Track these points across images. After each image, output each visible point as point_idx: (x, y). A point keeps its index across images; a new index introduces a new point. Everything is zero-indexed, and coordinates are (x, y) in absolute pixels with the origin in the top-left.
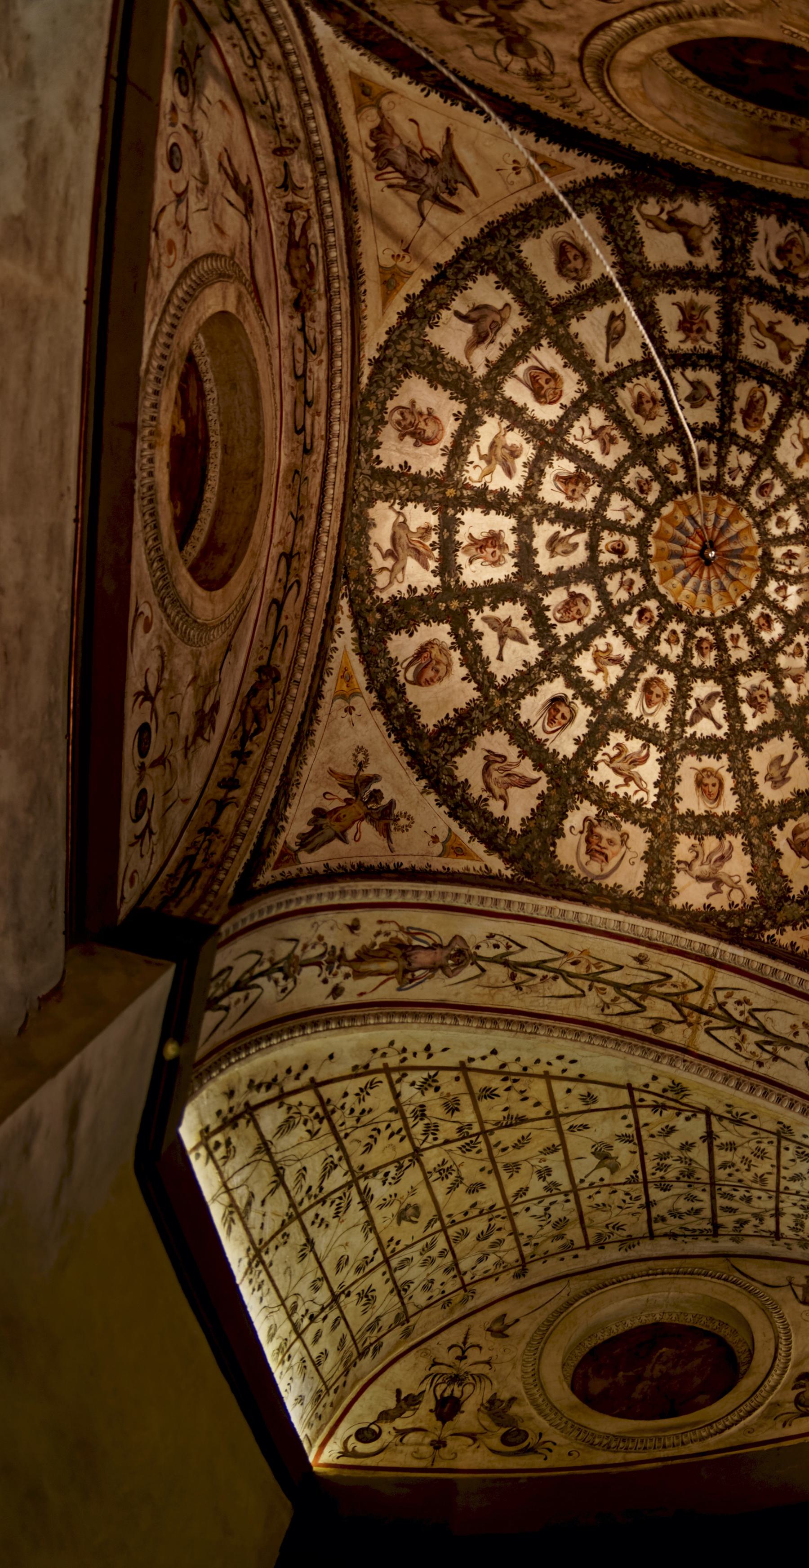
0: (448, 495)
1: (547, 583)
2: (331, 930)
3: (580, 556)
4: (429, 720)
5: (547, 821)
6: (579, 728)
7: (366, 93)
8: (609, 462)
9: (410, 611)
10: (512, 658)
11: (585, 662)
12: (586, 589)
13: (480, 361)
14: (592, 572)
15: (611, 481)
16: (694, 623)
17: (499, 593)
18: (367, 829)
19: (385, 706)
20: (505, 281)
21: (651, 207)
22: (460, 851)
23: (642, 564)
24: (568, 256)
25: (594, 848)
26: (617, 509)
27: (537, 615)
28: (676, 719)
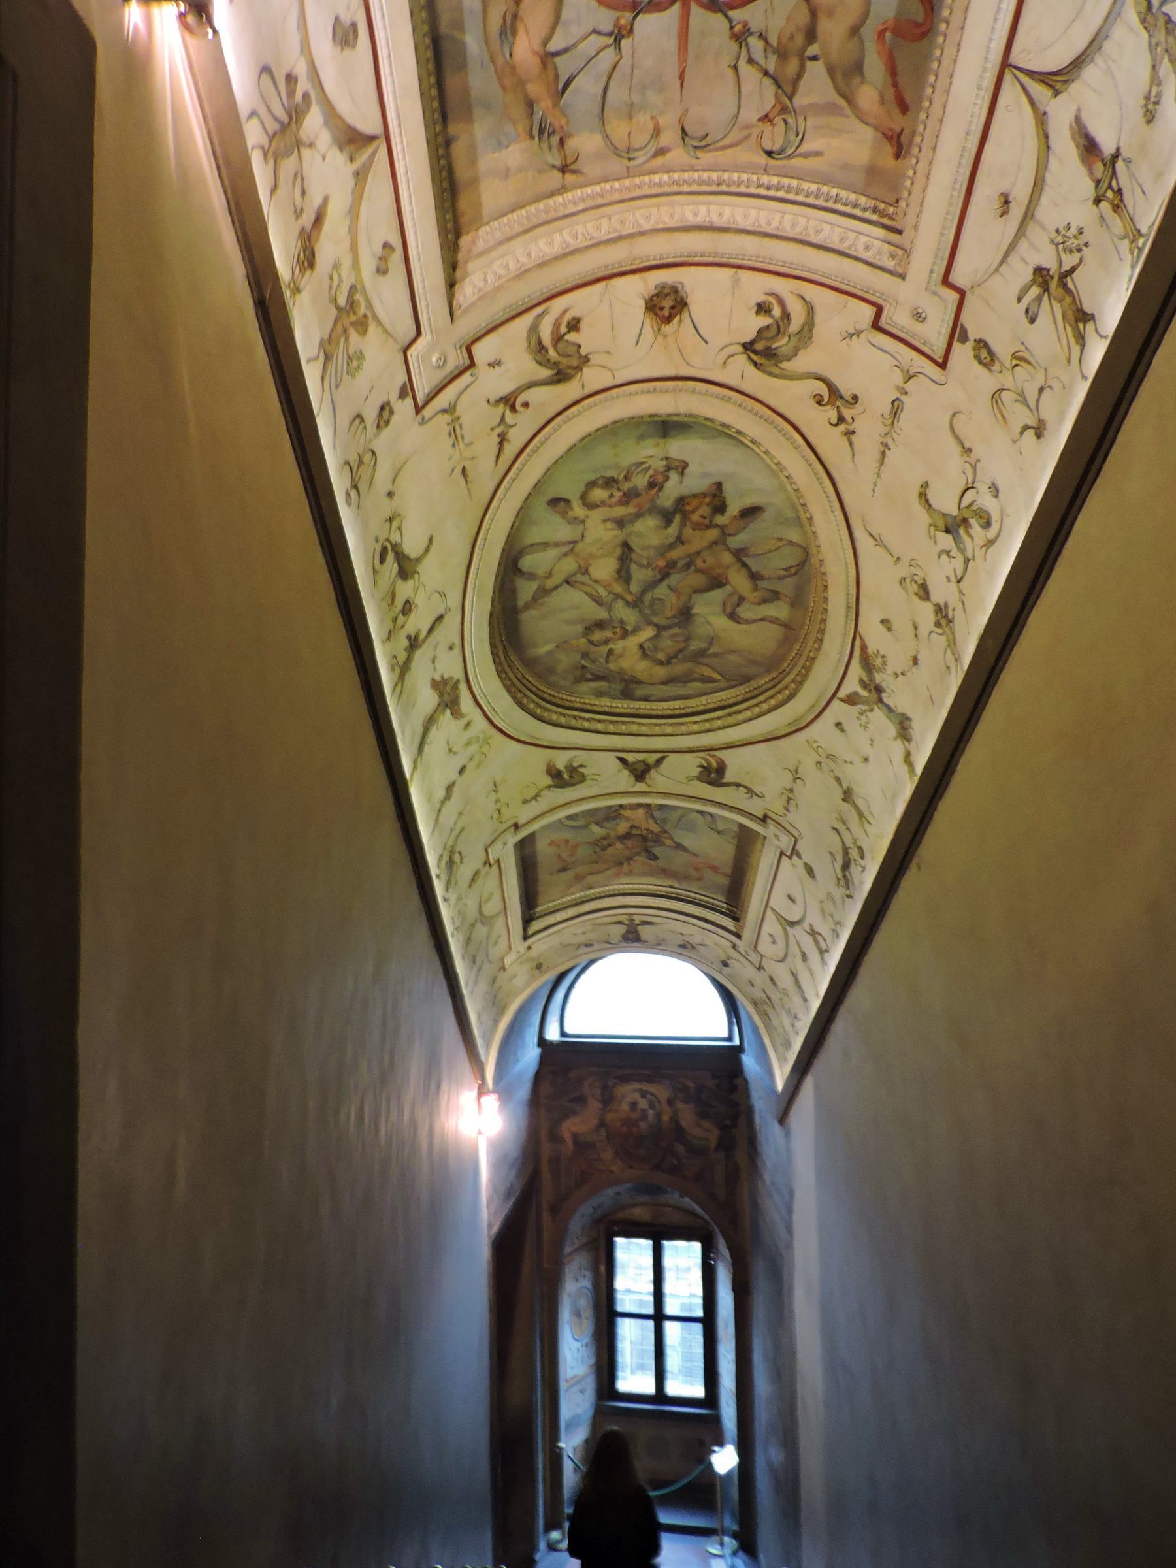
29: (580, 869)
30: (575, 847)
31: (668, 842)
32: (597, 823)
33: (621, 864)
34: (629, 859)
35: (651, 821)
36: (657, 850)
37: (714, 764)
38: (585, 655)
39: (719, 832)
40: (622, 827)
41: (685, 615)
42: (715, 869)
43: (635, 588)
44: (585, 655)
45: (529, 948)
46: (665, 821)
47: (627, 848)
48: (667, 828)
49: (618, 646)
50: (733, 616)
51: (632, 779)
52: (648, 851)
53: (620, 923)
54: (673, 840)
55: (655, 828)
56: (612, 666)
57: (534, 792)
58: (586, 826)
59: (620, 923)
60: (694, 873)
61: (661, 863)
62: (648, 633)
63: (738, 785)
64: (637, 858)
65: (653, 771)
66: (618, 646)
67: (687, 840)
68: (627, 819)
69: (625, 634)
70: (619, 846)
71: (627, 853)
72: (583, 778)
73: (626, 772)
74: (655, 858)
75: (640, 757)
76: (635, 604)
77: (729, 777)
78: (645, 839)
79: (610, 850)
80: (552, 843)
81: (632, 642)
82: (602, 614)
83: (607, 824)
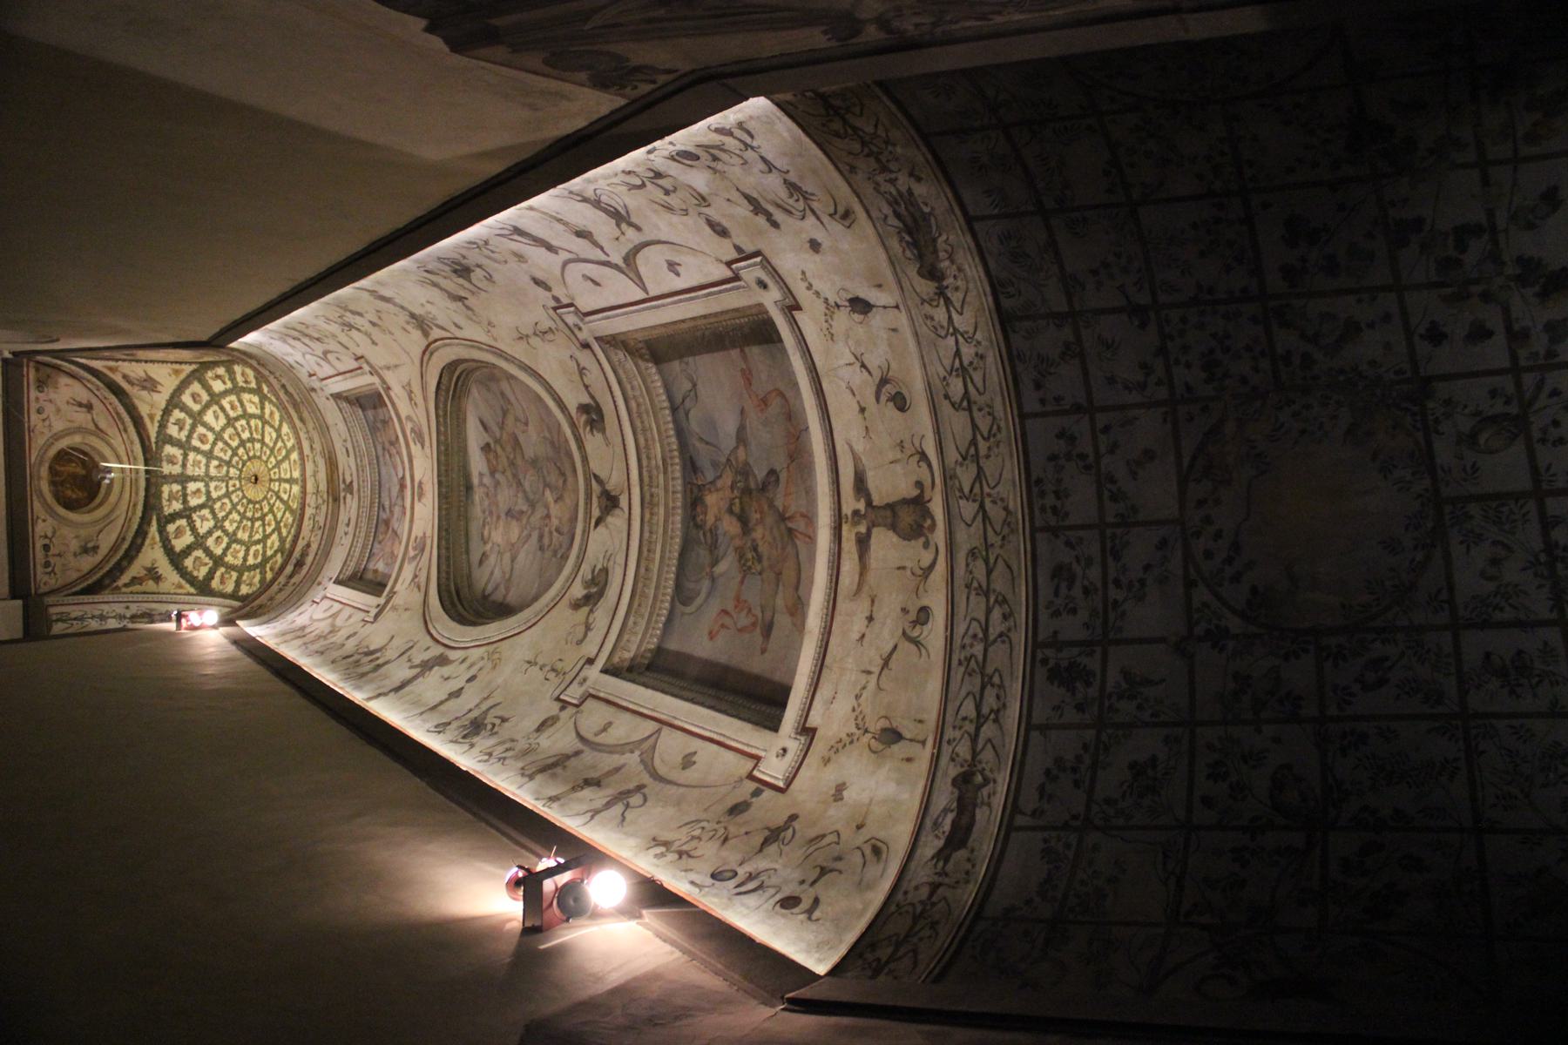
0: (183, 479)
1: (215, 501)
2: (119, 608)
3: (224, 491)
4: (178, 549)
5: (210, 575)
6: (224, 545)
7: (110, 369)
8: (227, 458)
9: (173, 517)
10: (203, 527)
11: (227, 524)
12: (226, 500)
13: (183, 436)
14: (228, 495)
15: (229, 464)
16: (255, 503)
17: (202, 507)
18: (151, 582)
19: (164, 547)
20: (182, 410)
21: (210, 374)
22: (180, 587)
23: (240, 489)
24: (195, 397)
25: (222, 582)
26: (233, 472)
27: (213, 512)
28: (250, 536)
29: (780, 602)
30: (739, 601)
31: (741, 453)
32: (715, 562)
33: (790, 530)
34: (782, 518)
35: (719, 483)
36: (760, 473)
37: (584, 418)
38: (555, 552)
39: (695, 385)
40: (730, 526)
41: (534, 462)
42: (747, 375)
43: (525, 508)
44: (555, 552)
45: (807, 731)
46: (715, 464)
47: (761, 521)
48: (723, 460)
49: (555, 522)
50: (526, 424)
51: (617, 511)
52: (764, 488)
53: (863, 542)
54: (737, 448)
55: (727, 479)
56: (565, 529)
57: (582, 629)
58: (713, 580)
59: (863, 542)
60: (775, 405)
61: (780, 463)
62: (548, 493)
63: (587, 387)
64: (779, 503)
65: (608, 487)
66: (555, 522)
67: (729, 426)
68: (718, 519)
69: (548, 516)
70: (758, 534)
71: (769, 520)
72: (605, 571)
73: (610, 519)
74: (772, 472)
75: (595, 500)
76: (533, 505)
77: (586, 400)
78: (747, 491)
79: (763, 548)
80: (712, 636)
81: (555, 510)
82: (535, 535)
83: (721, 550)
